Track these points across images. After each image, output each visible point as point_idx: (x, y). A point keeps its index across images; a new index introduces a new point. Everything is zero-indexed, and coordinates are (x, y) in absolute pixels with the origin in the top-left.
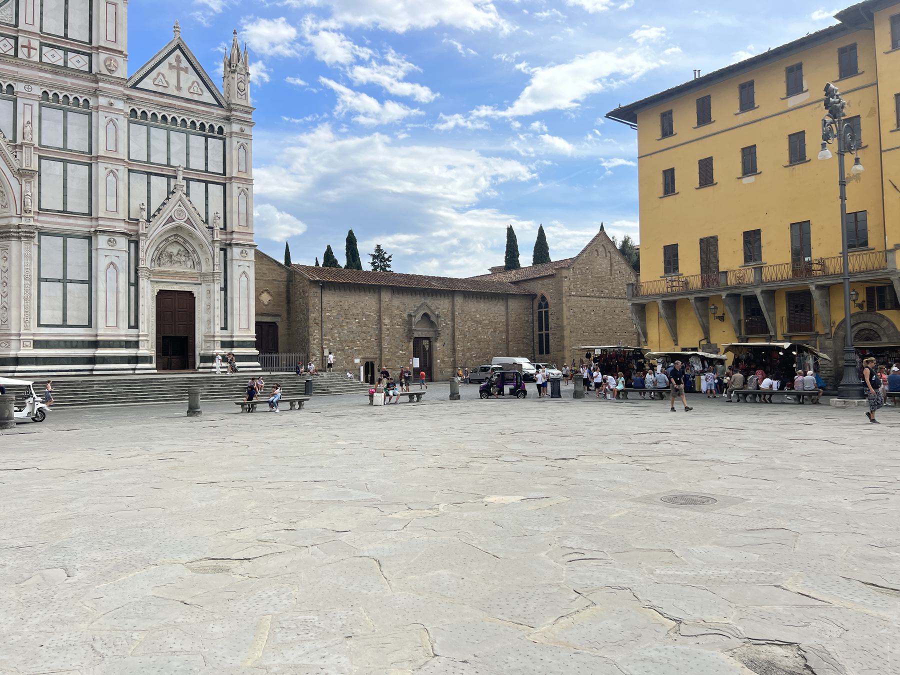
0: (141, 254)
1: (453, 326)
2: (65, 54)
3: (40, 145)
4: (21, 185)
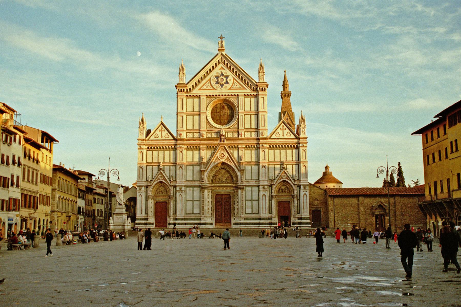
0: (273, 191)
2: (251, 133)
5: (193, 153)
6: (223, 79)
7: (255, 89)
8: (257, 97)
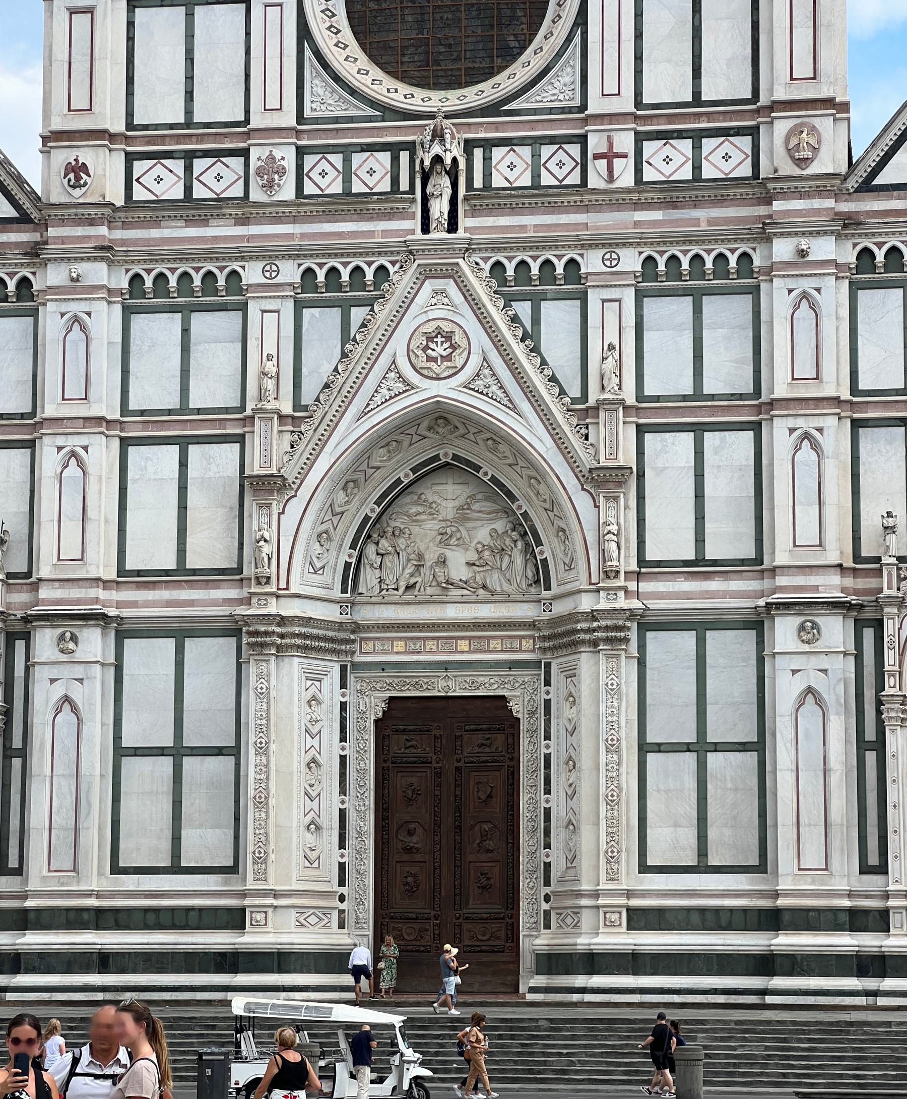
0: (890, 658)
2: (697, 147)
3: (640, 397)
4: (598, 507)
5: (186, 331)
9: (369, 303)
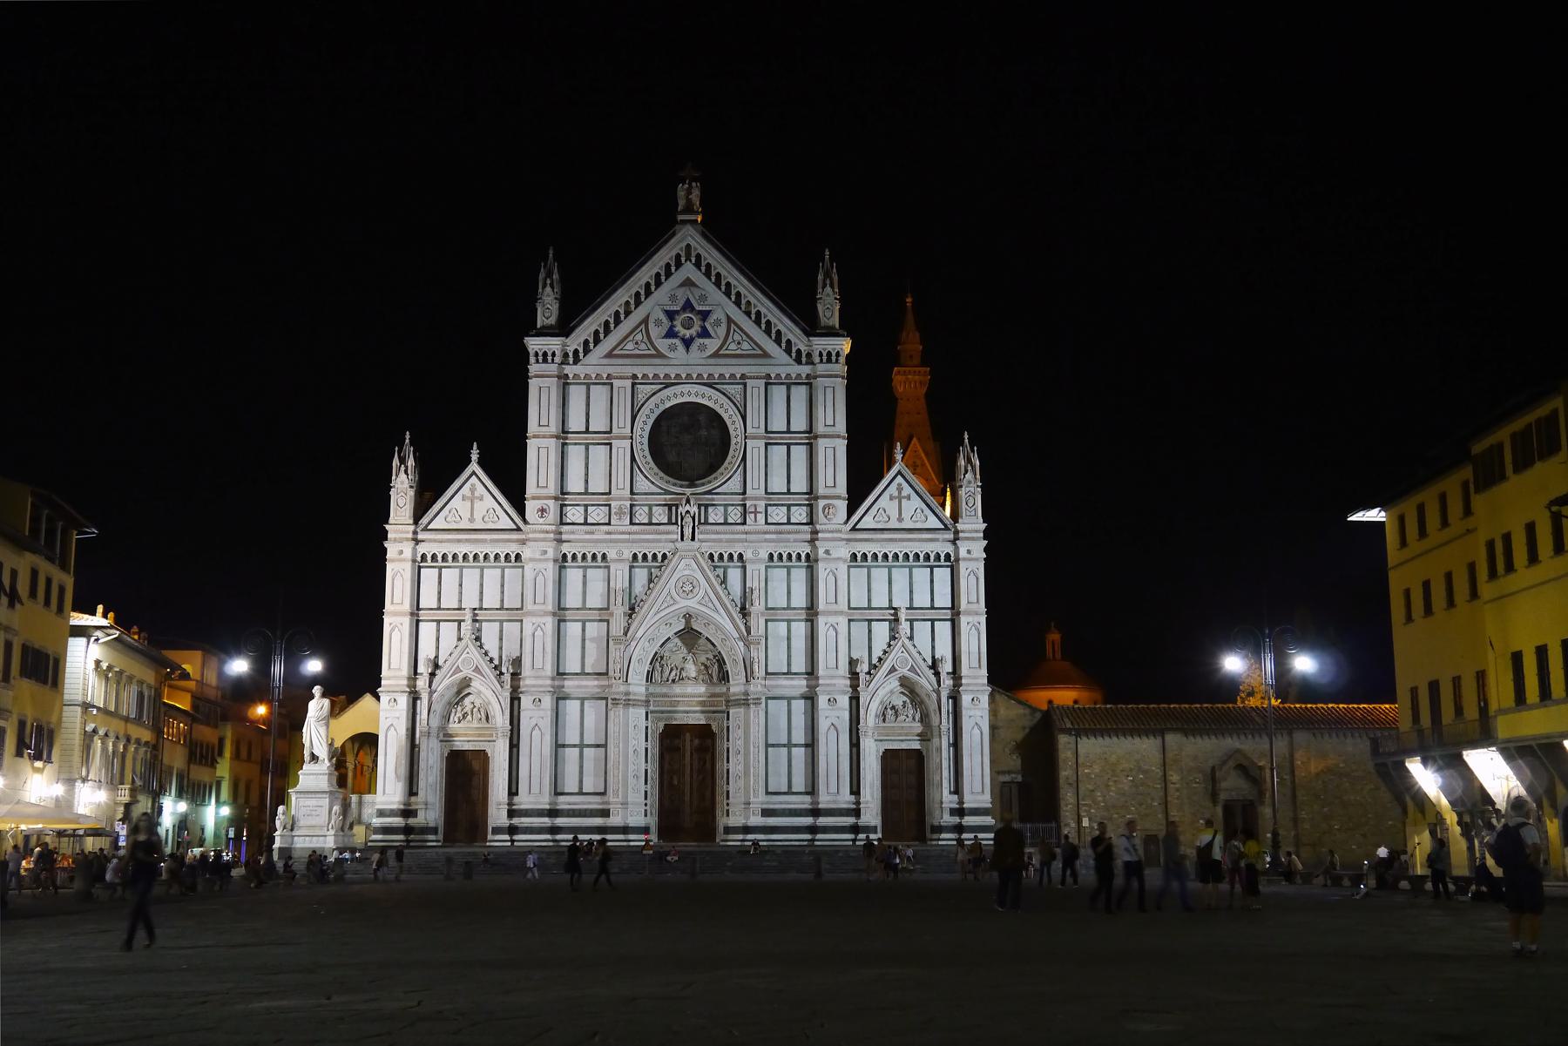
0: (862, 712)
1: (1293, 782)
2: (789, 510)
3: (767, 609)
5: (585, 576)
6: (691, 318)
7: (804, 360)
8: (810, 385)
9: (660, 567)
